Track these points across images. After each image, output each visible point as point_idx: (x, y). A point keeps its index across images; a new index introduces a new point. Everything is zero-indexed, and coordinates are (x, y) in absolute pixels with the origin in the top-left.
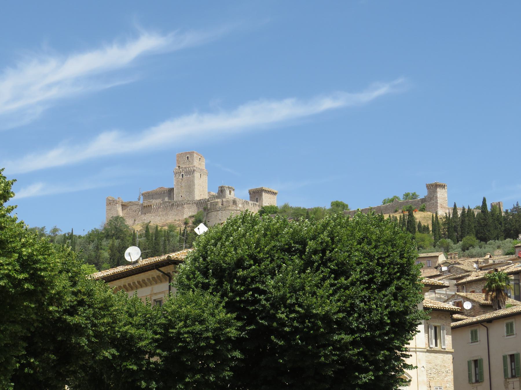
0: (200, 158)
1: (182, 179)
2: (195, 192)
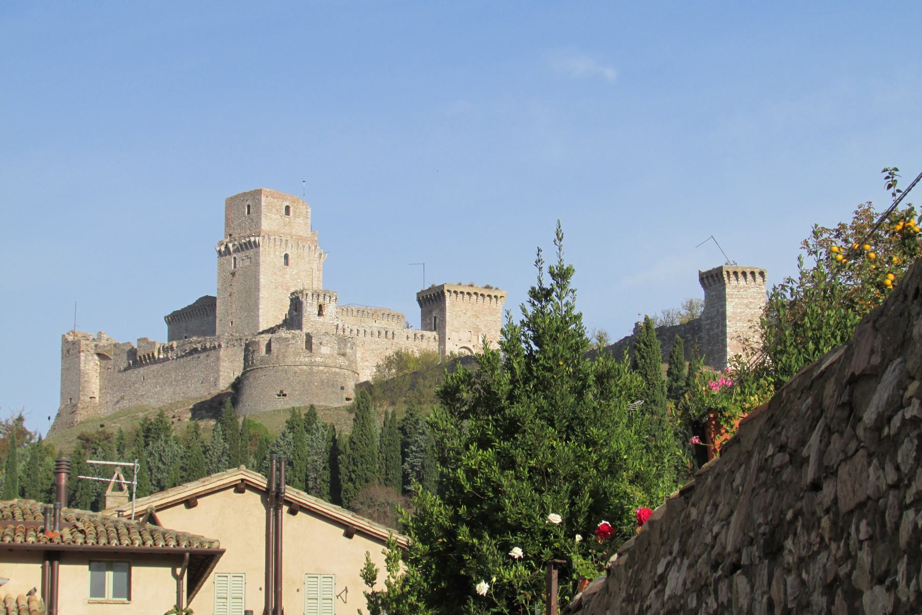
0: (287, 208)
1: (233, 274)
2: (258, 310)
